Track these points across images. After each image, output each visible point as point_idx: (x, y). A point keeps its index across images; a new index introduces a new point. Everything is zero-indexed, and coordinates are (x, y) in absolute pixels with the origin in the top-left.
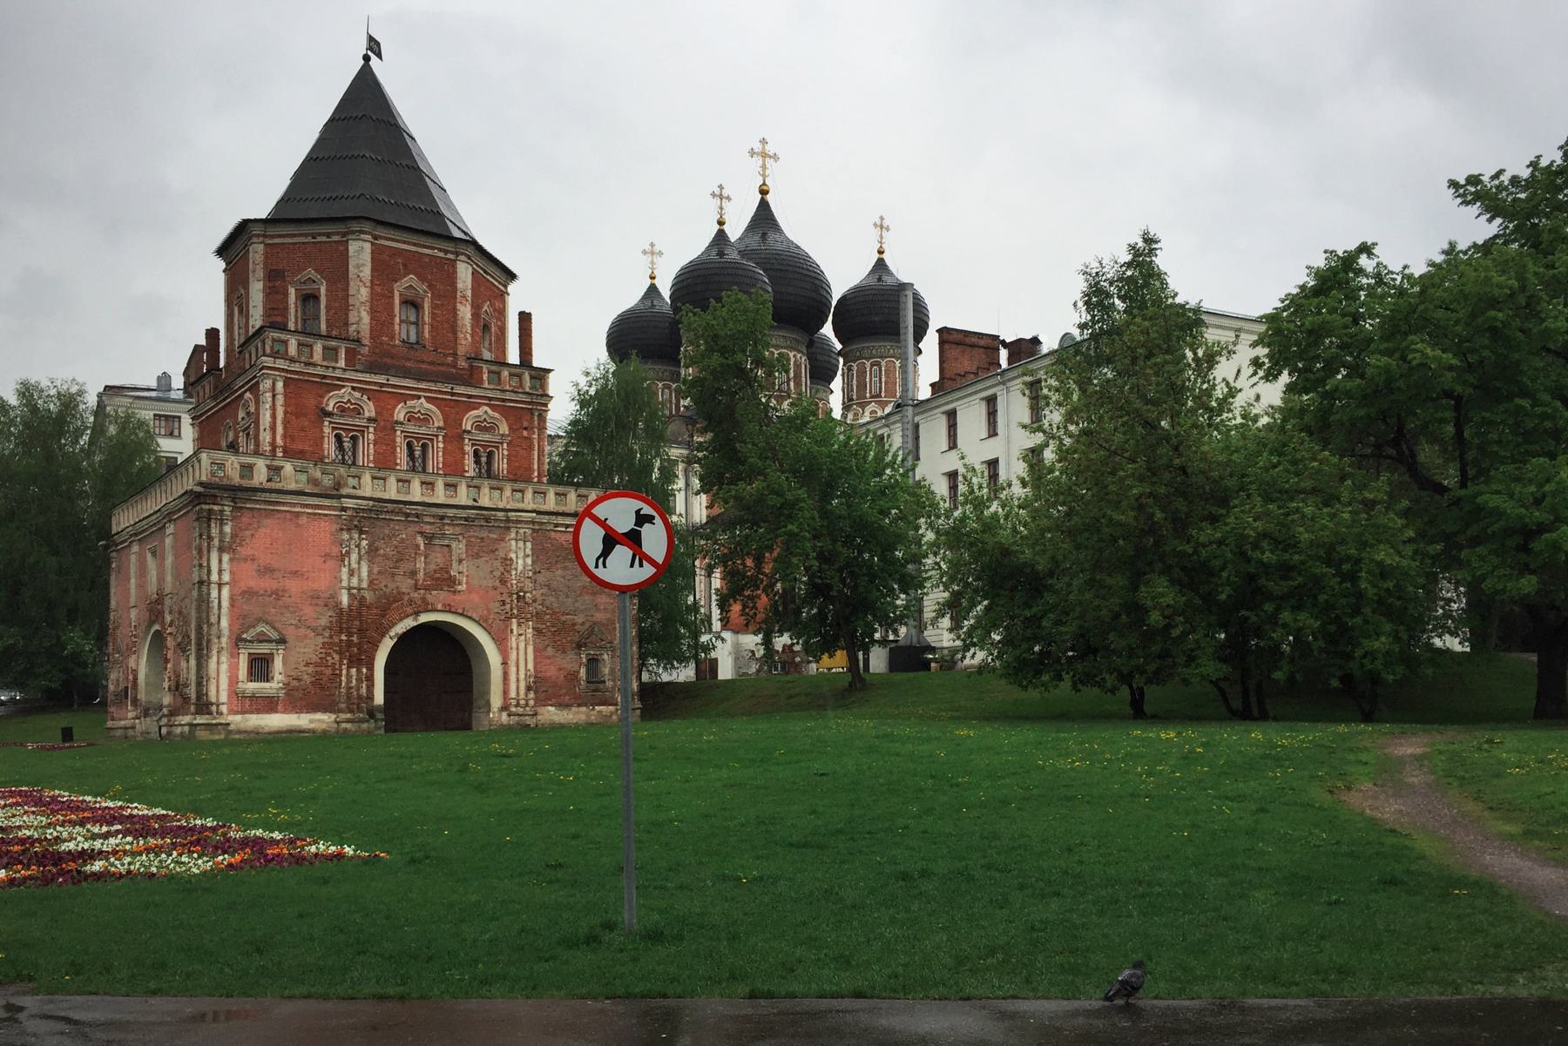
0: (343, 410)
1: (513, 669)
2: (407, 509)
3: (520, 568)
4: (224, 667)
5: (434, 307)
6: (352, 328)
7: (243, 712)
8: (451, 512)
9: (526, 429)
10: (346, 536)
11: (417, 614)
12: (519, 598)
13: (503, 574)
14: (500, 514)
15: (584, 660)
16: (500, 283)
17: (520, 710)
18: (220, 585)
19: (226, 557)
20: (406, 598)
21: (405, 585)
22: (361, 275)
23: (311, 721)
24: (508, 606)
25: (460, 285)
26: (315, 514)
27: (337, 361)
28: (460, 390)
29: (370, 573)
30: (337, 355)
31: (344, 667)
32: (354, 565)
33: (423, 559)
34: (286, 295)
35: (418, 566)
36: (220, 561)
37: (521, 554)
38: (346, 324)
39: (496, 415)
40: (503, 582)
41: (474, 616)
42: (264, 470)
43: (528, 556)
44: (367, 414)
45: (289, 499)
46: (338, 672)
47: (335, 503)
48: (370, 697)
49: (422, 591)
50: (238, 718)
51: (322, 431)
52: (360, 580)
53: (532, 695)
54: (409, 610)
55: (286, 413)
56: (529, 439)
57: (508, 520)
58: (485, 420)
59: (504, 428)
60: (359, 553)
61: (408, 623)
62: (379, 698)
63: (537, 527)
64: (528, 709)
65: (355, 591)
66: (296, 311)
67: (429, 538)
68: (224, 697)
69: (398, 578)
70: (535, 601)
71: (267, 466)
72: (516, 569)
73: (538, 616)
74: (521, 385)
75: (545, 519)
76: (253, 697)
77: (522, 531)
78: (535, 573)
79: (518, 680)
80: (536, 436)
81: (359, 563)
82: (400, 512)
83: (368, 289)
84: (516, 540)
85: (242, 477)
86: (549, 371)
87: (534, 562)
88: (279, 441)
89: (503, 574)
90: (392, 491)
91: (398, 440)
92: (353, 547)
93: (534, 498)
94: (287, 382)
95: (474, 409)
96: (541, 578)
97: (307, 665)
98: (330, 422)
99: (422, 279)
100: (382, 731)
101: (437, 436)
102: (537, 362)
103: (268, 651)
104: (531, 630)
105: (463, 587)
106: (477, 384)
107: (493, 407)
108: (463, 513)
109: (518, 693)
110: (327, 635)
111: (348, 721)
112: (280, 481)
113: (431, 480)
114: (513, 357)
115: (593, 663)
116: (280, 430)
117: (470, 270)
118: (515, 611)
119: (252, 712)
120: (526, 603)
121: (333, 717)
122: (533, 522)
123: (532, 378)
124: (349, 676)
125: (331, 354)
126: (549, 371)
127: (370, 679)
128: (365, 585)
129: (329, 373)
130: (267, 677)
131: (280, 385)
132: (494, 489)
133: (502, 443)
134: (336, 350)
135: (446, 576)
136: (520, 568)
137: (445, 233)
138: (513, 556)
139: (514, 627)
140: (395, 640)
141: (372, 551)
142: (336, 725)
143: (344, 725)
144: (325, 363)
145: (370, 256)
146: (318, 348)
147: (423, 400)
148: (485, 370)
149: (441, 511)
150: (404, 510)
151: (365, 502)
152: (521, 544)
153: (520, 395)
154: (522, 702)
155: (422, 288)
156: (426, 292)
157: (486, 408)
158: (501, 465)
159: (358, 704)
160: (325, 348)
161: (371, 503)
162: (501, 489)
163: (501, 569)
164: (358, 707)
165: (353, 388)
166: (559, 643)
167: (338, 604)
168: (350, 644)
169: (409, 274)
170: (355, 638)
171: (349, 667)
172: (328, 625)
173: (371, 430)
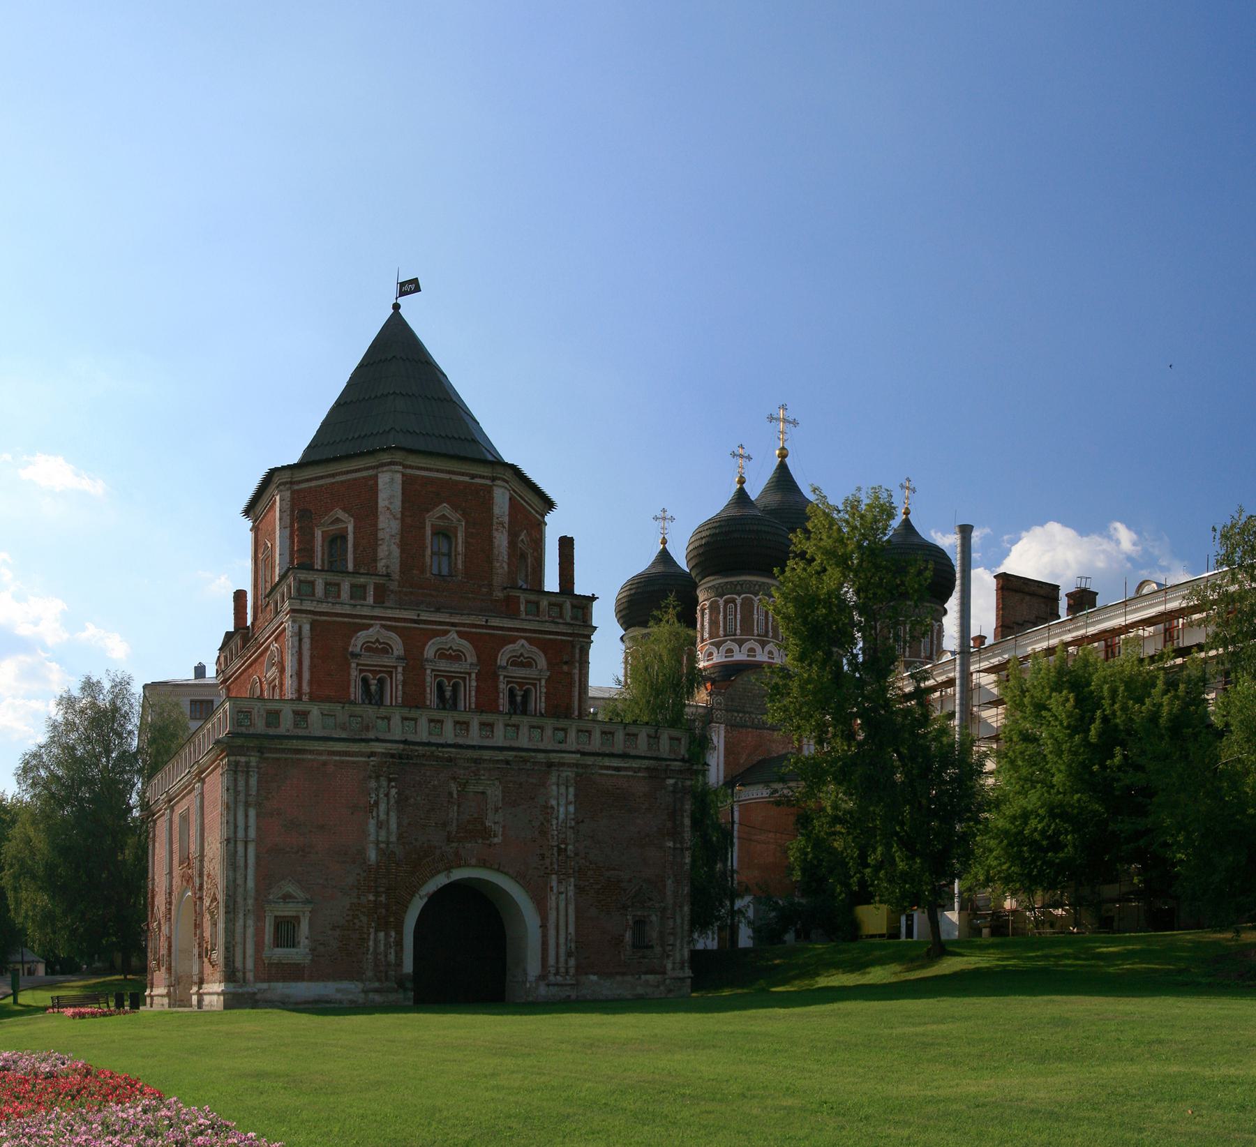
1: (552, 932)
2: (440, 752)
3: (562, 816)
4: (250, 931)
6: (380, 564)
7: (269, 980)
8: (487, 754)
9: (566, 663)
10: (373, 784)
11: (448, 869)
12: (560, 850)
13: (542, 824)
14: (541, 756)
15: (631, 922)
18: (246, 843)
22: (391, 507)
23: (338, 990)
24: (548, 861)
26: (342, 762)
27: (365, 599)
28: (495, 622)
29: (399, 825)
30: (365, 593)
31: (372, 930)
32: (383, 817)
33: (455, 808)
35: (450, 816)
36: (247, 816)
37: (563, 802)
38: (375, 560)
39: (534, 649)
42: (291, 715)
43: (571, 803)
44: (396, 653)
46: (366, 936)
48: (399, 963)
49: (454, 845)
50: (265, 986)
51: (349, 674)
55: (312, 657)
56: (570, 674)
59: (542, 662)
60: (388, 804)
61: (441, 880)
63: (581, 771)
65: (382, 846)
68: (250, 964)
70: (576, 854)
71: (294, 712)
72: (557, 819)
74: (561, 616)
75: (589, 760)
76: (279, 965)
77: (564, 774)
78: (577, 823)
80: (576, 671)
81: (388, 814)
83: (398, 522)
84: (558, 785)
85: (268, 725)
86: (593, 598)
87: (576, 809)
88: (306, 688)
89: (542, 824)
91: (428, 679)
92: (382, 796)
93: (578, 737)
94: (313, 625)
95: (510, 643)
97: (334, 928)
98: (358, 665)
99: (455, 507)
101: (470, 674)
102: (578, 590)
103: (294, 914)
104: (572, 888)
105: (496, 840)
111: (376, 991)
112: (307, 728)
114: (552, 583)
115: (640, 923)
116: (306, 675)
118: (556, 867)
119: (278, 981)
120: (567, 857)
121: (360, 985)
122: (577, 765)
123: (573, 606)
124: (378, 940)
125: (358, 592)
126: (593, 598)
127: (399, 944)
128: (393, 839)
129: (358, 611)
131: (306, 628)
132: (534, 727)
133: (540, 680)
134: (364, 587)
136: (562, 816)
137: (478, 457)
138: (554, 803)
139: (554, 884)
140: (425, 900)
141: (402, 801)
142: (362, 995)
143: (371, 995)
144: (352, 602)
145: (400, 487)
148: (522, 600)
151: (395, 746)
152: (563, 790)
153: (561, 626)
155: (454, 516)
156: (459, 520)
157: (523, 641)
158: (539, 702)
159: (386, 972)
160: (352, 586)
161: (401, 746)
162: (542, 728)
165: (383, 626)
170: (383, 899)
171: (376, 931)
173: (400, 669)
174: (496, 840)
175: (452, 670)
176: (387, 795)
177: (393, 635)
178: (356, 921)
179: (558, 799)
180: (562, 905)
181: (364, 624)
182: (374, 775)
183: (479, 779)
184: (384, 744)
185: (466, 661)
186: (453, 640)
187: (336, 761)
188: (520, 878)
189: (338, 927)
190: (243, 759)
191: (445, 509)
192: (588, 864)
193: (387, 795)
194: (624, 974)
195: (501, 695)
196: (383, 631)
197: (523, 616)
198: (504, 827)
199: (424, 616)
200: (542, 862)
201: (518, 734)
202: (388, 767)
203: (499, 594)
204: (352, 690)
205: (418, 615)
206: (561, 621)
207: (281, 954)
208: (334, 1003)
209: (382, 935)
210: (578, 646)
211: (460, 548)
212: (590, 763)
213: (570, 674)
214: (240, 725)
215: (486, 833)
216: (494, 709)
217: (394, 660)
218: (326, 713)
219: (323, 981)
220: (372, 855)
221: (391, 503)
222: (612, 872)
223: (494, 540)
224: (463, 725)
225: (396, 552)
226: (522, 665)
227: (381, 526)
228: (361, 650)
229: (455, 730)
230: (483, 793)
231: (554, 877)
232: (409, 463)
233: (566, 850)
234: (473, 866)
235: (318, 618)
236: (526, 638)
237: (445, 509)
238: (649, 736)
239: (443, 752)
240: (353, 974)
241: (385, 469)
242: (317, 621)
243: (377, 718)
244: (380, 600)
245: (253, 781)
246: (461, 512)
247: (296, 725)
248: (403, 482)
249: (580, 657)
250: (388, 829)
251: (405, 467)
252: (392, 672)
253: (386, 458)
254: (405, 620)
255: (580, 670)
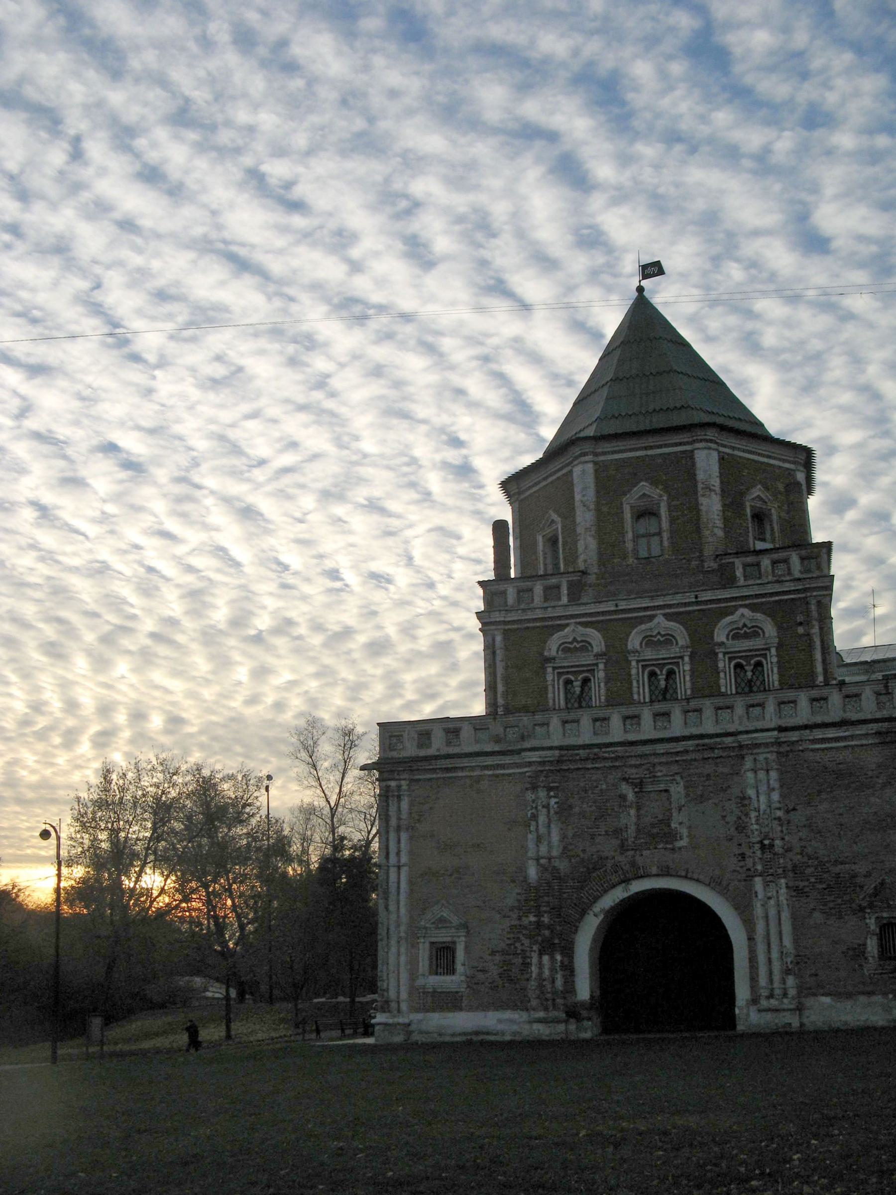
0: (567, 650)
2: (605, 753)
3: (763, 807)
5: (670, 509)
8: (660, 748)
9: (801, 624)
10: (530, 796)
11: (626, 881)
12: (763, 847)
14: (728, 740)
16: (784, 461)
17: (773, 1002)
19: (404, 836)
20: (609, 863)
21: (608, 847)
23: (500, 1021)
24: (749, 862)
25: (701, 476)
27: (559, 599)
29: (564, 837)
30: (560, 593)
32: (542, 830)
34: (535, 544)
36: (399, 842)
37: (763, 788)
38: (577, 557)
39: (759, 616)
40: (741, 828)
41: (701, 877)
43: (773, 789)
44: (596, 650)
45: (465, 762)
47: (516, 759)
49: (631, 853)
50: (420, 1016)
52: (550, 846)
53: (791, 981)
54: (615, 879)
55: (506, 668)
57: (741, 747)
58: (745, 625)
59: (770, 630)
61: (617, 895)
62: (584, 990)
64: (785, 1001)
65: (542, 861)
66: (545, 558)
67: (639, 785)
68: (404, 995)
69: (598, 839)
71: (444, 729)
73: (796, 870)
74: (790, 574)
75: (794, 736)
77: (761, 757)
78: (788, 812)
79: (770, 961)
80: (815, 630)
82: (596, 758)
84: (755, 771)
85: (420, 746)
90: (585, 734)
94: (506, 633)
96: (798, 818)
97: (493, 953)
98: (554, 668)
99: (654, 483)
100: (589, 1030)
101: (682, 657)
104: (783, 890)
105: (682, 843)
106: (729, 581)
107: (753, 608)
108: (680, 746)
109: (771, 981)
110: (515, 916)
111: (539, 1021)
112: (459, 745)
113: (636, 713)
116: (500, 688)
117: (715, 455)
118: (759, 867)
119: (434, 1011)
121: (524, 1016)
123: (802, 559)
125: (551, 592)
127: (569, 969)
129: (551, 613)
130: (450, 970)
131: (499, 638)
133: (768, 649)
134: (558, 587)
135: (666, 830)
136: (763, 807)
138: (751, 792)
140: (601, 917)
141: (564, 811)
143: (536, 1026)
144: (546, 605)
145: (592, 476)
146: (538, 589)
147: (660, 619)
149: (647, 749)
150: (602, 755)
151: (549, 753)
152: (762, 775)
153: (787, 584)
154: (777, 992)
155: (655, 492)
159: (554, 1000)
161: (557, 753)
163: (737, 812)
164: (554, 1005)
165: (579, 623)
166: (831, 905)
167: (526, 878)
168: (539, 925)
169: (637, 483)
170: (546, 919)
171: (541, 954)
172: (516, 904)
173: (601, 666)
174: (682, 843)
175: (661, 656)
176: (547, 806)
177: (589, 631)
178: (518, 945)
179: (757, 787)
180: (772, 912)
181: (559, 625)
182: (529, 786)
183: (655, 776)
184: (537, 753)
185: (677, 643)
186: (661, 623)
187: (490, 776)
188: (715, 884)
189: (498, 952)
190: (393, 784)
191: (644, 487)
192: (805, 859)
193: (547, 806)
194: (870, 994)
195: (722, 675)
196: (580, 629)
197: (742, 582)
198: (690, 827)
199: (623, 605)
200: (742, 863)
201: (701, 719)
202: (546, 777)
203: (712, 564)
204: (550, 695)
205: (617, 606)
206: (788, 578)
207: (435, 981)
208: (495, 1034)
209: (546, 958)
210: (814, 602)
211: (665, 525)
212: (794, 739)
213: (808, 635)
214: (391, 748)
215: (670, 836)
216: (714, 692)
217: (592, 658)
218: (478, 727)
219: (484, 1010)
220: (532, 872)
221: (584, 496)
222: (840, 867)
223: (702, 508)
224: (632, 719)
225: (593, 544)
226: (746, 636)
227: (579, 519)
228: (557, 652)
229: (624, 725)
230: (666, 791)
231: (758, 880)
232: (600, 450)
233: (772, 846)
234: (658, 875)
235: (509, 627)
236: (745, 606)
237: (644, 487)
238: (878, 694)
239: (608, 752)
240: (520, 1004)
241: (575, 463)
242: (509, 629)
243: (535, 725)
244: (574, 597)
245: (405, 805)
246: (661, 487)
247: (449, 743)
248: (596, 471)
249: (820, 614)
250: (549, 842)
251: (596, 454)
252: (594, 670)
253: (576, 450)
254: (603, 613)
255: (821, 629)
